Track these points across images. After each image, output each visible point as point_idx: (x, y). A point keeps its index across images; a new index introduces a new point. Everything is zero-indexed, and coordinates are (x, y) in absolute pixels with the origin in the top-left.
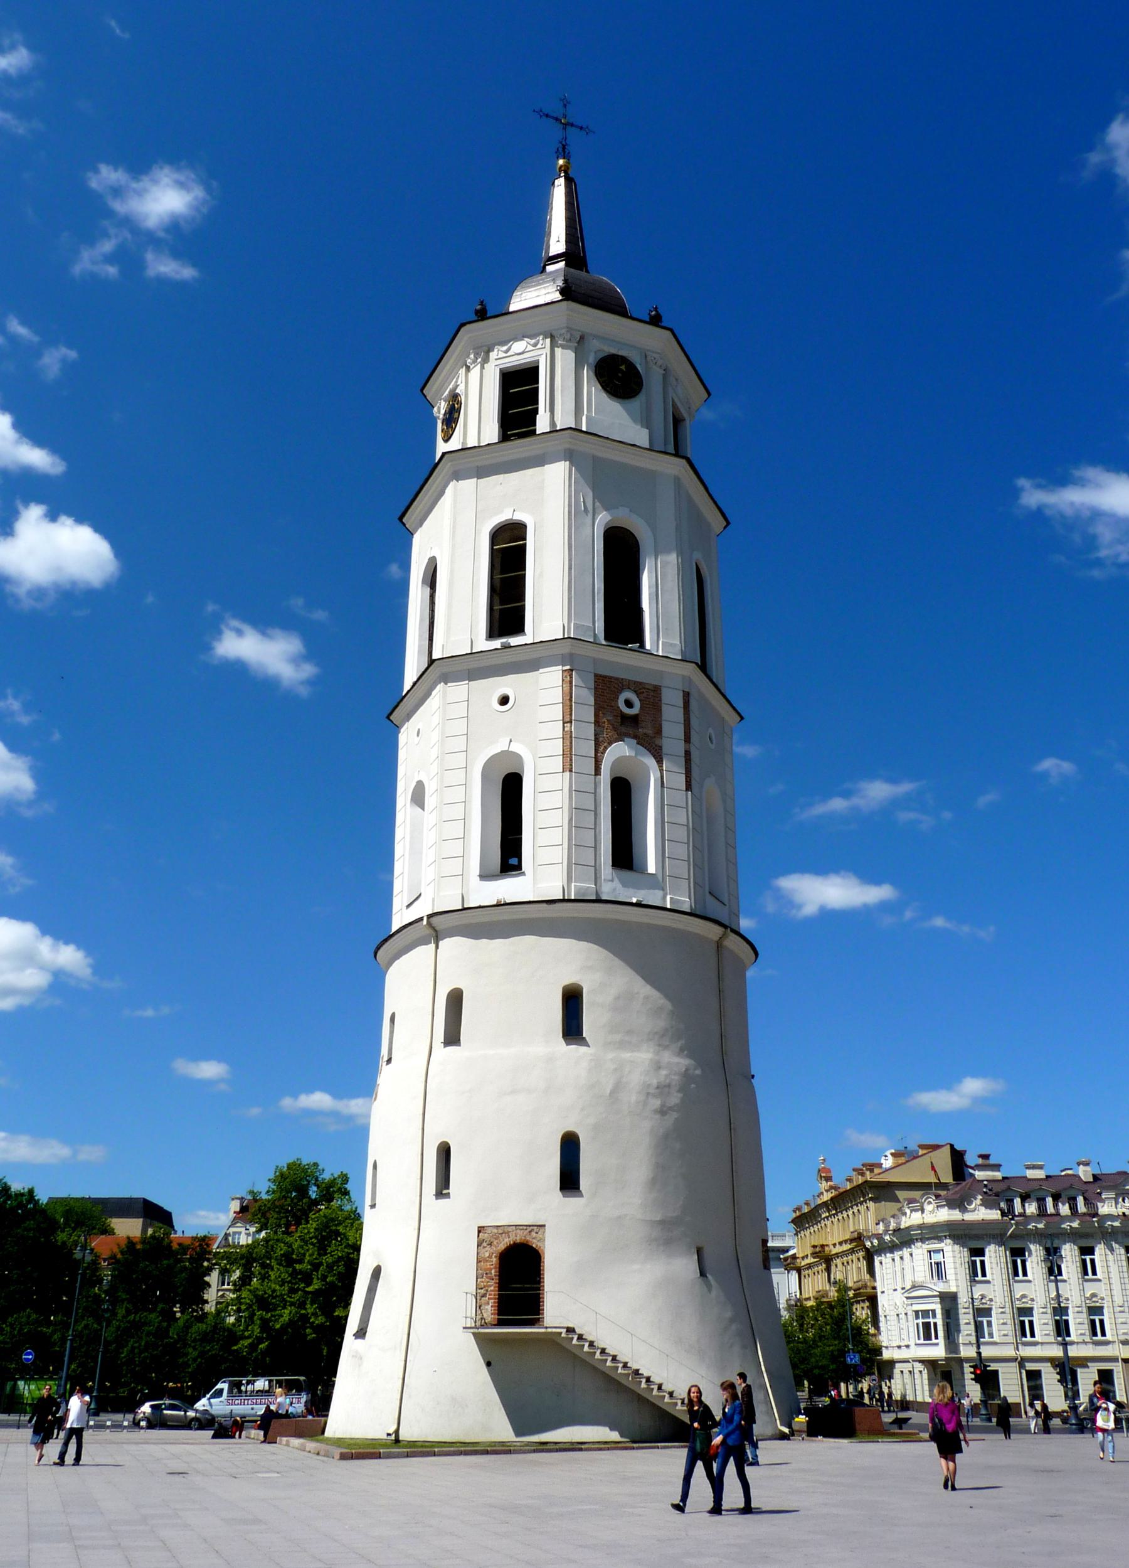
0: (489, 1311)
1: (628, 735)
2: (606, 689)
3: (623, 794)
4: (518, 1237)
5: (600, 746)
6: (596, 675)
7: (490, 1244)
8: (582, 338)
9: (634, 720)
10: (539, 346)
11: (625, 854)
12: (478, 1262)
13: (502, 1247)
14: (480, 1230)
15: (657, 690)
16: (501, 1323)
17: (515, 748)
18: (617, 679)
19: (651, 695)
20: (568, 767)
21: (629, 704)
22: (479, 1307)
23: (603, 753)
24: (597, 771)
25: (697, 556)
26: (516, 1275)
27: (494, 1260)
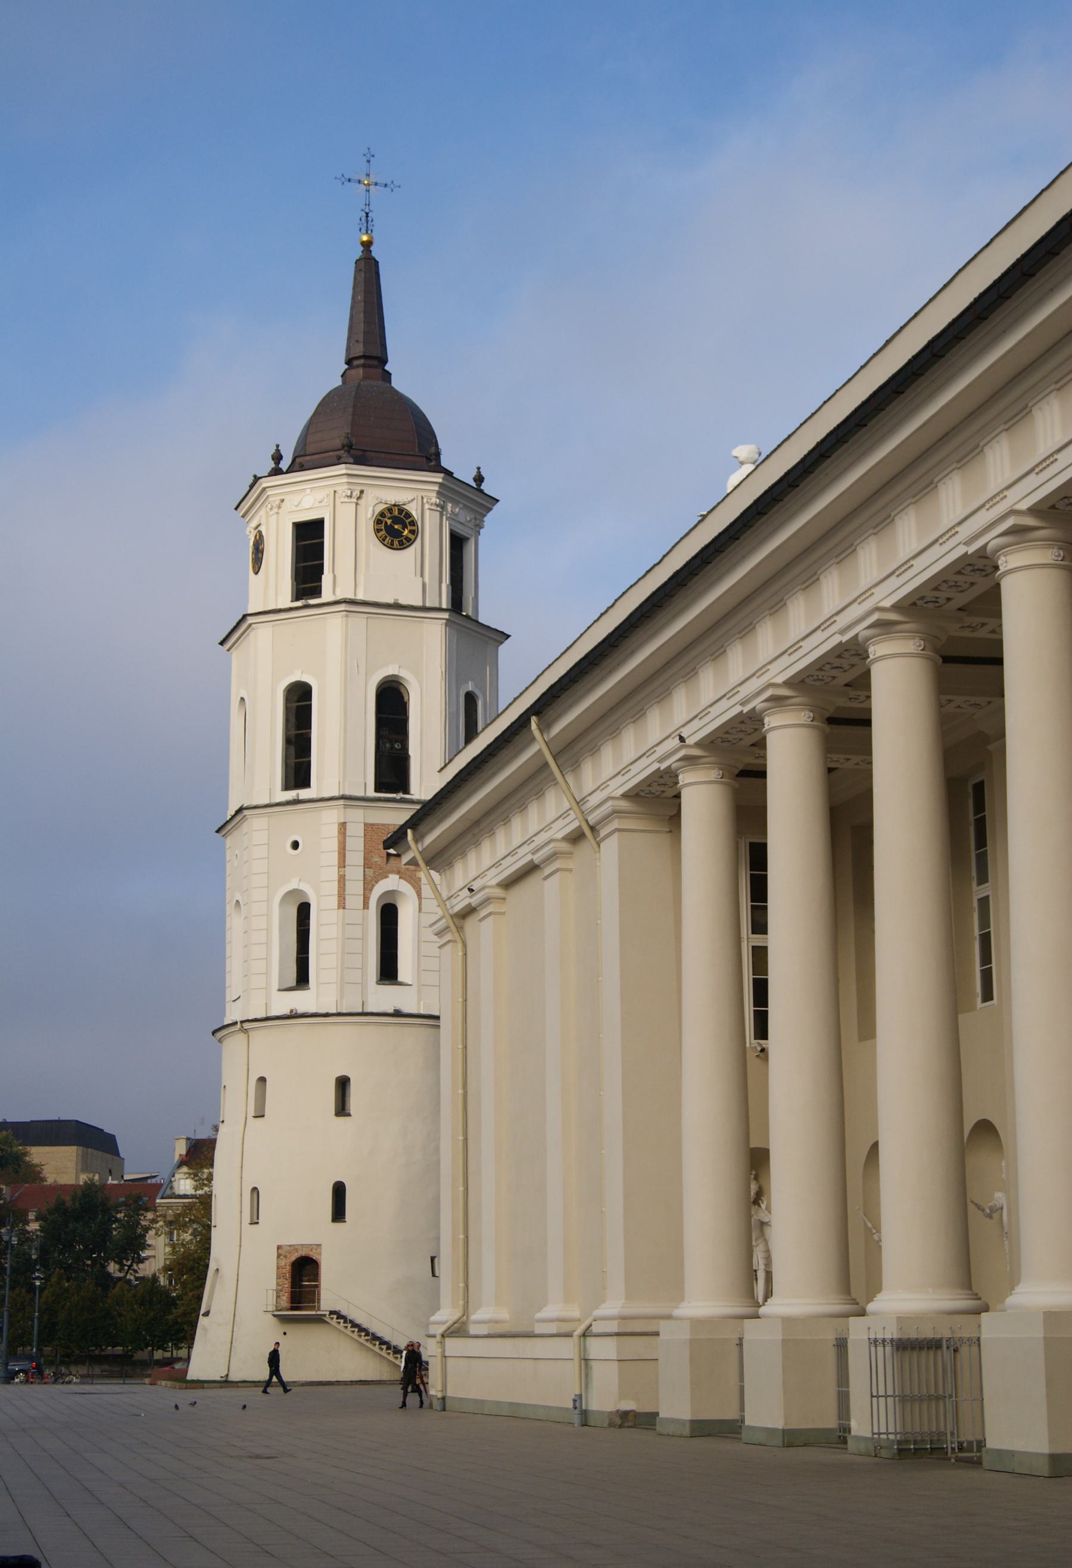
0: (285, 1300)
1: (392, 872)
4: (303, 1253)
5: (368, 887)
6: (365, 824)
7: (285, 1256)
8: (362, 492)
10: (324, 504)
11: (388, 971)
12: (278, 1268)
13: (293, 1258)
14: (279, 1247)
16: (292, 1309)
17: (303, 887)
18: (383, 825)
20: (342, 905)
22: (278, 1297)
23: (371, 890)
24: (366, 905)
25: (470, 687)
26: (302, 1274)
27: (288, 1268)
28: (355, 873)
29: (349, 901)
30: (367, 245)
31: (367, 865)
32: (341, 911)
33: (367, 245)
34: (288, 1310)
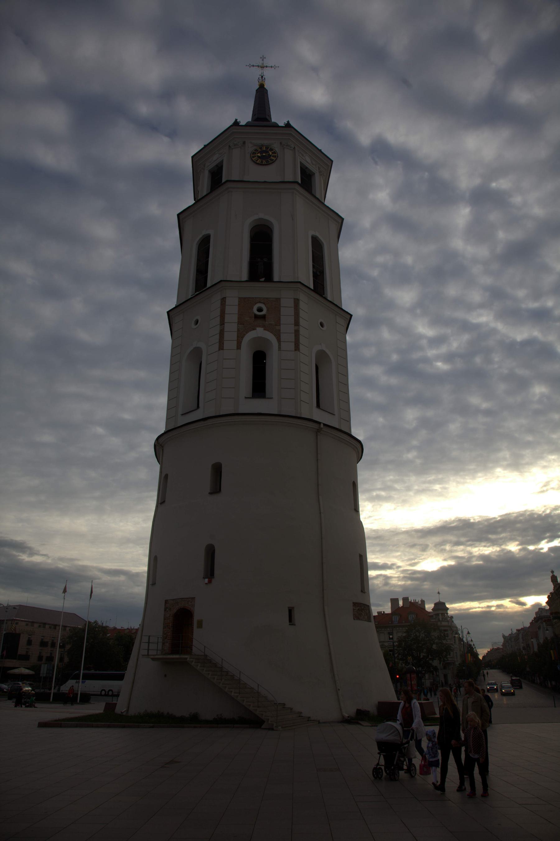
1: (260, 326)
2: (245, 304)
3: (259, 360)
6: (239, 298)
9: (264, 317)
12: (165, 619)
14: (166, 602)
15: (278, 300)
16: (172, 653)
19: (275, 305)
20: (221, 348)
21: (260, 310)
23: (242, 338)
24: (239, 347)
28: (231, 328)
29: (226, 345)
30: (262, 86)
31: (240, 322)
32: (221, 351)
33: (262, 86)
34: (170, 654)
